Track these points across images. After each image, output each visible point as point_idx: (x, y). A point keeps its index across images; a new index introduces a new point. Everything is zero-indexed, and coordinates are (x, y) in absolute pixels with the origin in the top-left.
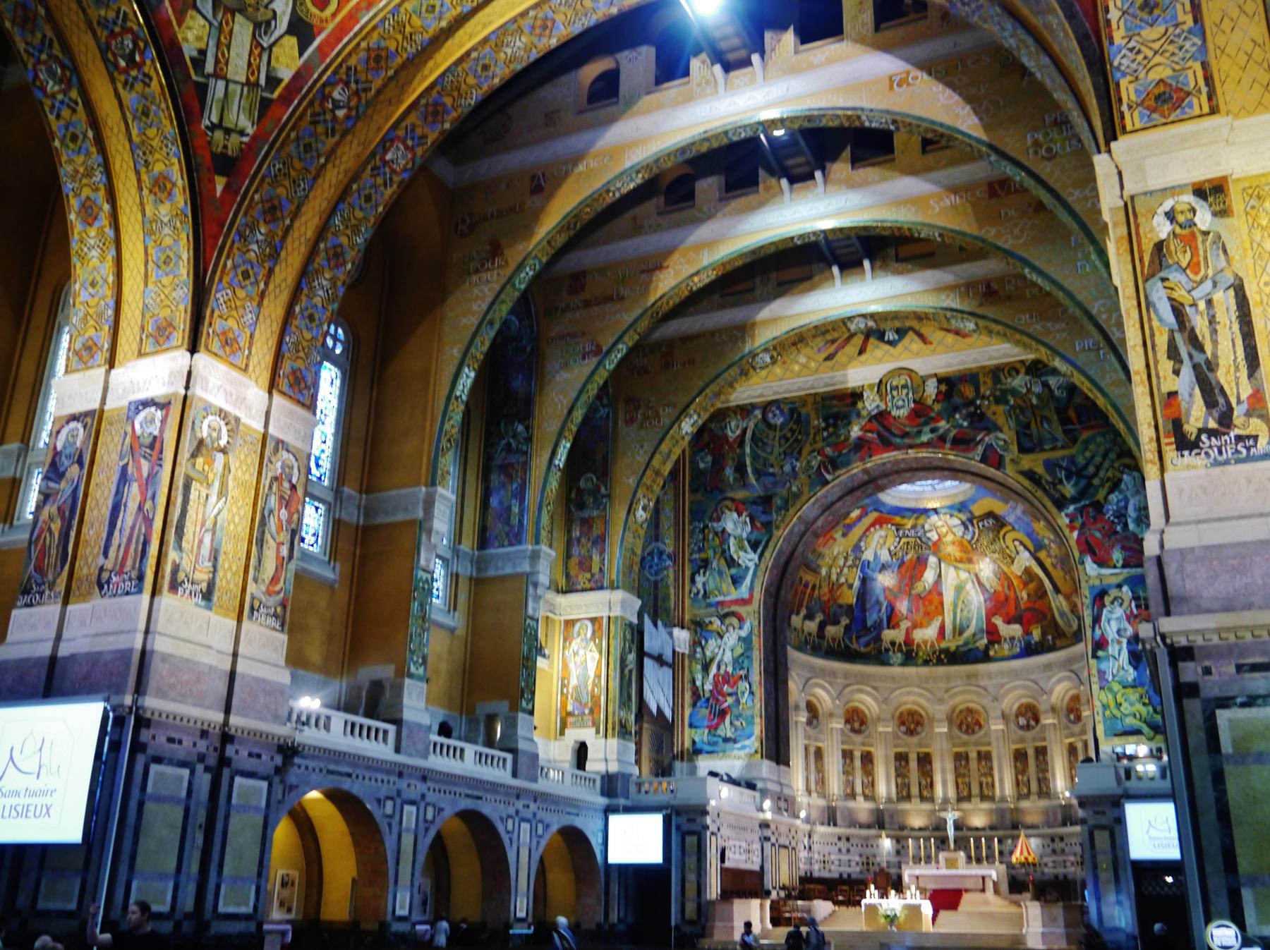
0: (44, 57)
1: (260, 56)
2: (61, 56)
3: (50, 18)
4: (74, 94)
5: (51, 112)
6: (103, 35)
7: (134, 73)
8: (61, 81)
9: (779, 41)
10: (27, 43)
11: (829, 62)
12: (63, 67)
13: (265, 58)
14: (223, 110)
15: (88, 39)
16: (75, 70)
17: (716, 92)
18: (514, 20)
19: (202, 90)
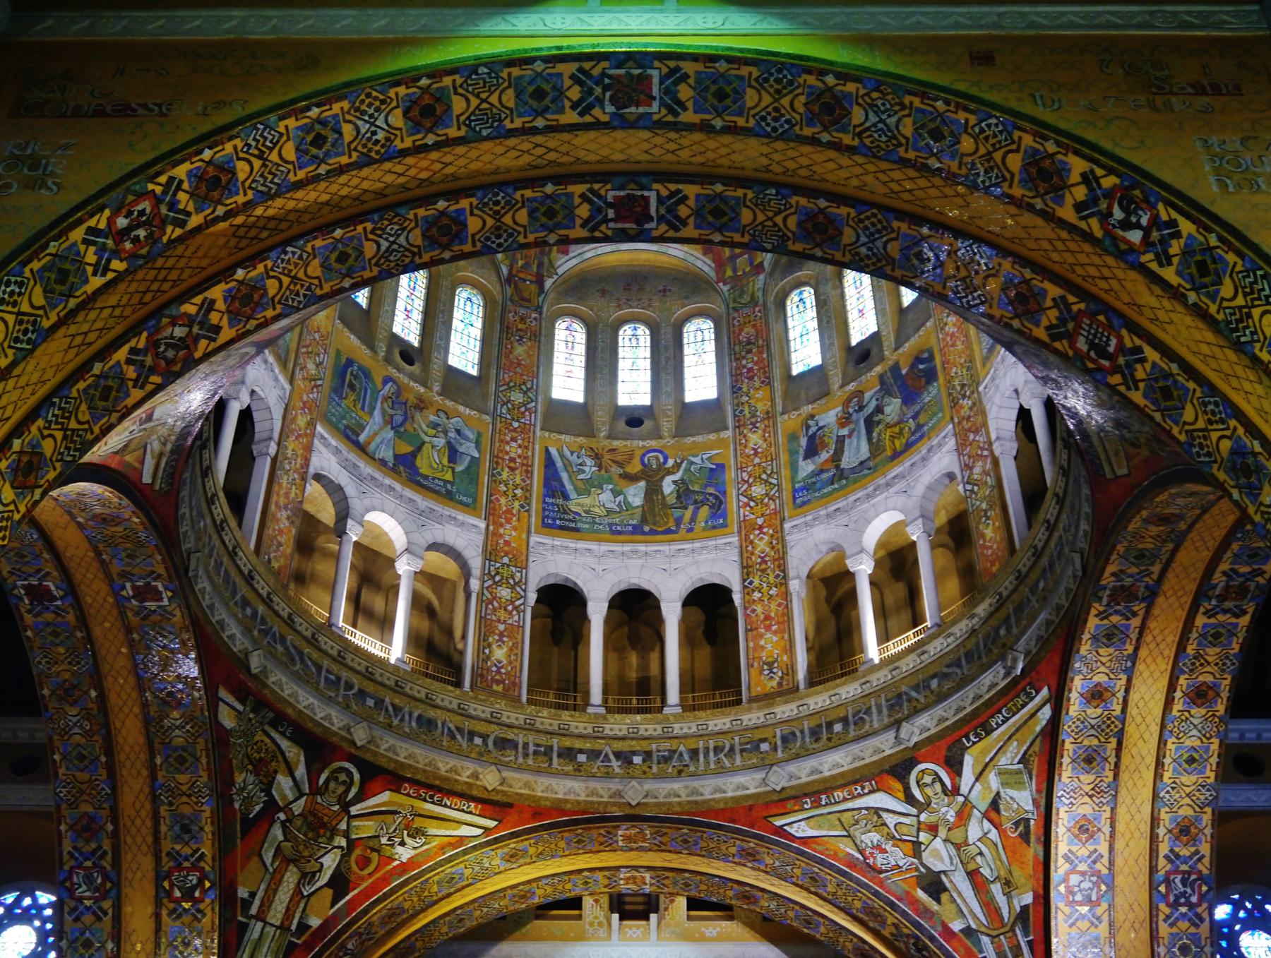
0: (88, 864)
1: (298, 903)
2: (109, 868)
3: (115, 835)
4: (107, 904)
5: (69, 914)
6: (167, 864)
7: (186, 905)
8: (96, 890)
9: (672, 901)
10: (75, 848)
11: (719, 938)
12: (106, 877)
13: (302, 905)
14: (254, 950)
15: (148, 863)
16: (118, 885)
17: (609, 937)
18: (504, 890)
19: (243, 928)
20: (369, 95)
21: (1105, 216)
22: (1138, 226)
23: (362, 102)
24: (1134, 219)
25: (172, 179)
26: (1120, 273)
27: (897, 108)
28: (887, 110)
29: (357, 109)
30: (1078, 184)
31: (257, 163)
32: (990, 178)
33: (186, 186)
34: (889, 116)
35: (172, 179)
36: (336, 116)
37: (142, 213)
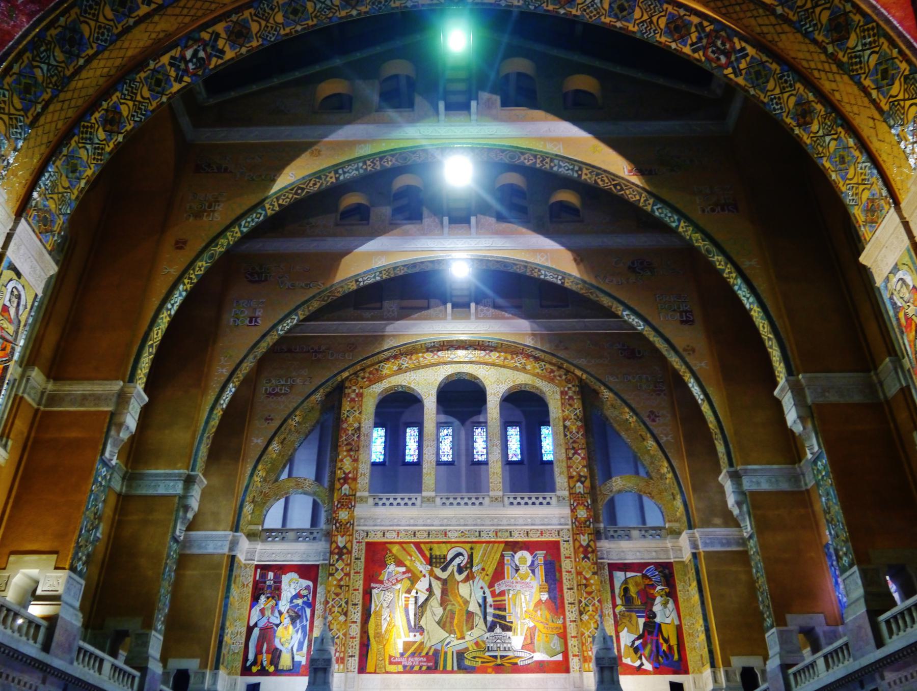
20: (591, 17)
21: (205, 44)
22: (191, 60)
23: (594, 16)
24: (194, 60)
25: (694, 51)
26: (180, 19)
27: (319, 14)
28: (323, 10)
29: (598, 13)
30: (224, 47)
31: (655, 19)
32: (261, 9)
33: (689, 42)
34: (321, 8)
35: (694, 51)
36: (610, 16)
37: (713, 52)
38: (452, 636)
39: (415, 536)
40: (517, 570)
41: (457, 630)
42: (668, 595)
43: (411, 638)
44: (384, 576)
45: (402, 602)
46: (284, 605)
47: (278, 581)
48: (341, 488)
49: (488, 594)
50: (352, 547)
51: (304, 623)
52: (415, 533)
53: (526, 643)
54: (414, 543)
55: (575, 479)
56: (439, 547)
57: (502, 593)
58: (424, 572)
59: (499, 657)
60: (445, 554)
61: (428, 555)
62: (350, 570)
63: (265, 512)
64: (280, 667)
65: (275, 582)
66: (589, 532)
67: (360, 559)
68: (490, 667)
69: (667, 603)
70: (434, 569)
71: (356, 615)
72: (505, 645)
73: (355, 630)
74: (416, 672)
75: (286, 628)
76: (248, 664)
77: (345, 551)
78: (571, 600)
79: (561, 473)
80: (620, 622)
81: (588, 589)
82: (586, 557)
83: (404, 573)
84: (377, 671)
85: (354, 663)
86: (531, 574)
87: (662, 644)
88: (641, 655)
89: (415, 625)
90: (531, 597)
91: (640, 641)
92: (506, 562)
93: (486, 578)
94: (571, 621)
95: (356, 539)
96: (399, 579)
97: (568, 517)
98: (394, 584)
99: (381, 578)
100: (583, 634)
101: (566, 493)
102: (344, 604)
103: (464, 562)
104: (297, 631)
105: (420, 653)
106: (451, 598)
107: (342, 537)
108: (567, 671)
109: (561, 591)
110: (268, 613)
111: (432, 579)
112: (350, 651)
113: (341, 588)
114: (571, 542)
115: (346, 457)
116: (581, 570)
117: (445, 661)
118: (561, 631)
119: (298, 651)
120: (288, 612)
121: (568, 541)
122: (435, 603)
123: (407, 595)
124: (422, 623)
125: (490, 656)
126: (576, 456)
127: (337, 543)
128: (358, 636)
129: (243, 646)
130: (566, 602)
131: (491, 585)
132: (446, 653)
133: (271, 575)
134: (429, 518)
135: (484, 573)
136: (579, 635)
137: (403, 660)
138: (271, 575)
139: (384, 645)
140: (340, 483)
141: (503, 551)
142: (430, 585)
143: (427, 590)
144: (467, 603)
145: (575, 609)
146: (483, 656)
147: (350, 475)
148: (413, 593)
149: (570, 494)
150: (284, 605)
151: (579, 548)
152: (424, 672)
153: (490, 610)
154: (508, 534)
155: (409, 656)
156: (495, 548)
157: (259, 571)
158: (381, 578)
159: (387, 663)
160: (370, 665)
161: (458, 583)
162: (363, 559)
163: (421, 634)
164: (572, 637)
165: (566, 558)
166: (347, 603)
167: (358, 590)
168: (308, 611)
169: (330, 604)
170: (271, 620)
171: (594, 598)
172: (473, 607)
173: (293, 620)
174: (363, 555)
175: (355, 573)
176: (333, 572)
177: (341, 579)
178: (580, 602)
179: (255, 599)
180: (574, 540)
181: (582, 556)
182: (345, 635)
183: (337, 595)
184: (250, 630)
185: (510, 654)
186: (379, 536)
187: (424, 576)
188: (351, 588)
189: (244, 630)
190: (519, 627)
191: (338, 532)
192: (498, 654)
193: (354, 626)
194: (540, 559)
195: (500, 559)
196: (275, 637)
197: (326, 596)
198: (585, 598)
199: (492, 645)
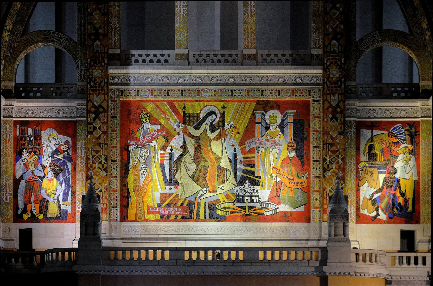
38: (205, 189)
39: (168, 95)
40: (267, 129)
41: (209, 184)
42: (411, 152)
43: (167, 190)
44: (139, 134)
45: (158, 159)
46: (46, 160)
47: (37, 136)
48: (93, 45)
49: (239, 151)
50: (107, 106)
51: (67, 176)
52: (168, 91)
53: (272, 196)
54: (168, 102)
55: (331, 36)
56: (192, 106)
57: (252, 151)
58: (178, 130)
59: (247, 208)
60: (198, 112)
61: (182, 114)
62: (107, 129)
63: (16, 67)
64: (49, 215)
65: (35, 138)
66: (340, 92)
67: (116, 117)
68: (239, 216)
69: (410, 160)
70: (188, 127)
71: (116, 171)
72: (253, 198)
73: (116, 184)
74: (172, 221)
75: (50, 181)
76: (19, 212)
77: (101, 110)
78: (316, 158)
79: (317, 29)
80: (362, 177)
81: (334, 148)
82: (334, 117)
83: (159, 131)
84: (137, 220)
85: (116, 212)
86: (280, 133)
87: (399, 197)
88: (378, 206)
89: (170, 179)
90: (279, 153)
91: (379, 194)
92: (256, 121)
93: (238, 136)
94: (315, 177)
95: (111, 97)
96: (154, 136)
97: (320, 76)
98: (151, 142)
99: (137, 135)
100: (325, 189)
101: (320, 51)
102: (103, 161)
103: (217, 121)
104: (61, 184)
105: (176, 204)
106: (204, 155)
107: (97, 96)
108: (309, 221)
109: (309, 148)
110: (32, 167)
111: (186, 137)
112: (112, 202)
113: (100, 146)
114: (321, 102)
115: (95, 10)
116: (328, 130)
117: (198, 211)
118: (305, 186)
119: (63, 201)
120: (50, 166)
121: (318, 101)
122: (188, 159)
123: (162, 152)
124: (177, 177)
125: (239, 207)
126: (335, 11)
127: (92, 102)
128: (119, 189)
129: (12, 196)
130: (312, 159)
131: (242, 143)
132: (199, 204)
133: (30, 131)
134: (182, 77)
135: (236, 131)
136: (321, 189)
137: (161, 210)
138: (30, 131)
139: (143, 197)
140: (91, 39)
141: (254, 110)
142: (184, 142)
143: (181, 147)
144: (219, 159)
145: (319, 166)
146: (232, 206)
147: (101, 31)
148: (169, 149)
149: (324, 52)
150: (46, 160)
151: (328, 109)
152: (180, 221)
153: (240, 166)
154: (260, 93)
155: (166, 206)
156: (247, 107)
157: (18, 126)
158: (137, 135)
159: (146, 212)
160: (131, 214)
161: (211, 140)
162: (119, 118)
163: (176, 188)
164: (315, 191)
165: (315, 117)
166: (106, 159)
167: (116, 147)
168: (70, 165)
169: (91, 161)
170: (35, 174)
171: (338, 156)
172: (225, 163)
173: (56, 174)
174: (119, 113)
175: (112, 131)
176: (92, 130)
177: (100, 137)
178: (325, 160)
179: (18, 154)
180: (324, 101)
181: (331, 116)
182: (106, 188)
183: (97, 152)
184: (17, 182)
185: (258, 206)
186: (133, 95)
187: (178, 134)
188: (109, 145)
189: (11, 182)
190: (266, 182)
191: (93, 90)
192: (247, 205)
193: (114, 180)
194: (290, 119)
195: (251, 118)
196: (41, 188)
197: (87, 153)
198: (330, 157)
199: (241, 198)
